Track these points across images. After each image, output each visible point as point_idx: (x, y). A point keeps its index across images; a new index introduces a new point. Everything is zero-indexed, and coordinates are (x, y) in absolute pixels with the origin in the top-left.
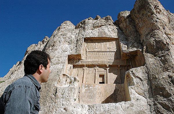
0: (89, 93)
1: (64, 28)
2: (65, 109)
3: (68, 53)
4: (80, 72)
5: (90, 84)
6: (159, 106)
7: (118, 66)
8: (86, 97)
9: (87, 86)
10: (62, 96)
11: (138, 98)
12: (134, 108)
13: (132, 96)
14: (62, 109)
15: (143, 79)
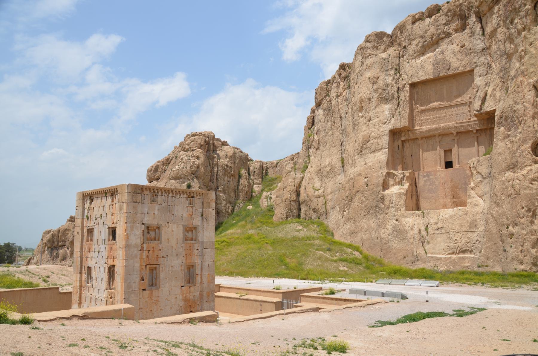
0: (430, 185)
1: (370, 55)
2: (397, 220)
3: (390, 127)
4: (414, 149)
5: (429, 172)
6: (490, 216)
7: (472, 131)
8: (426, 191)
9: (425, 174)
10: (391, 205)
11: (475, 202)
12: (467, 217)
13: (469, 201)
14: (395, 221)
15: (485, 176)
